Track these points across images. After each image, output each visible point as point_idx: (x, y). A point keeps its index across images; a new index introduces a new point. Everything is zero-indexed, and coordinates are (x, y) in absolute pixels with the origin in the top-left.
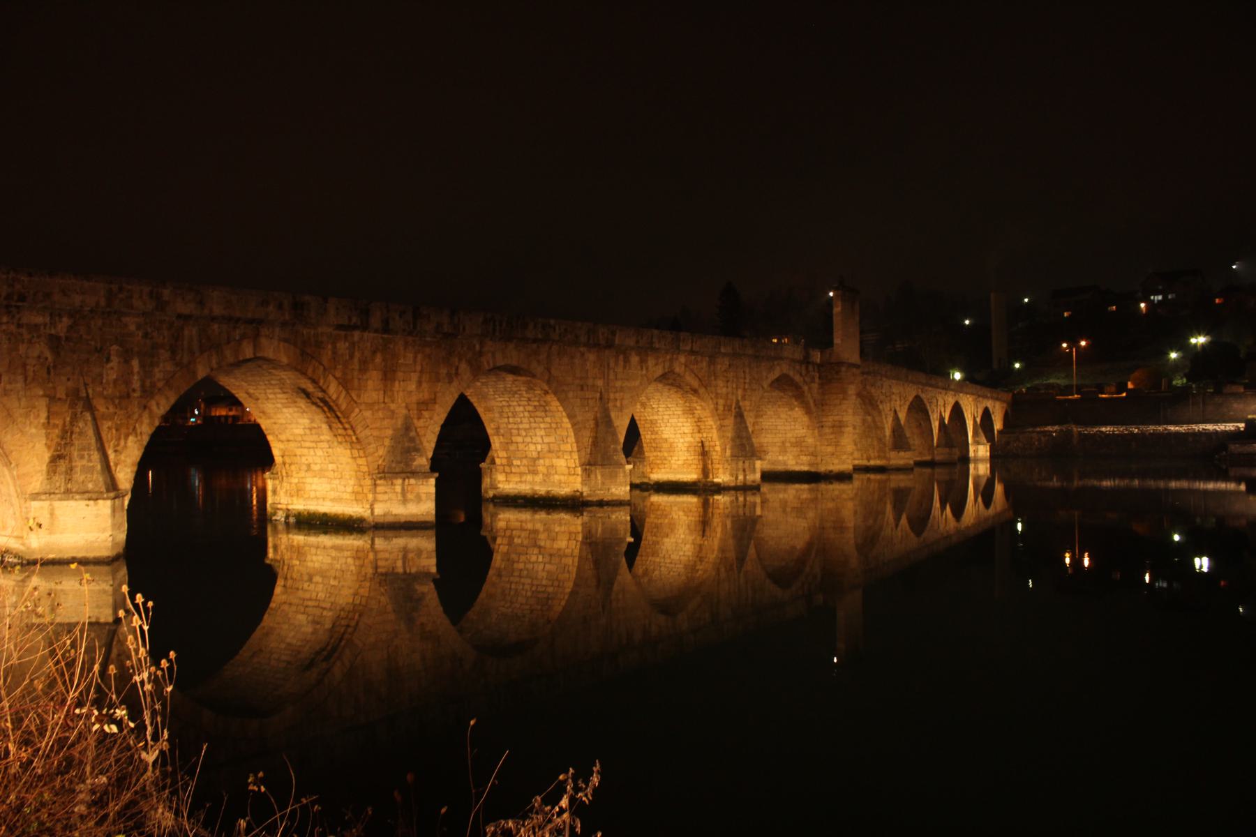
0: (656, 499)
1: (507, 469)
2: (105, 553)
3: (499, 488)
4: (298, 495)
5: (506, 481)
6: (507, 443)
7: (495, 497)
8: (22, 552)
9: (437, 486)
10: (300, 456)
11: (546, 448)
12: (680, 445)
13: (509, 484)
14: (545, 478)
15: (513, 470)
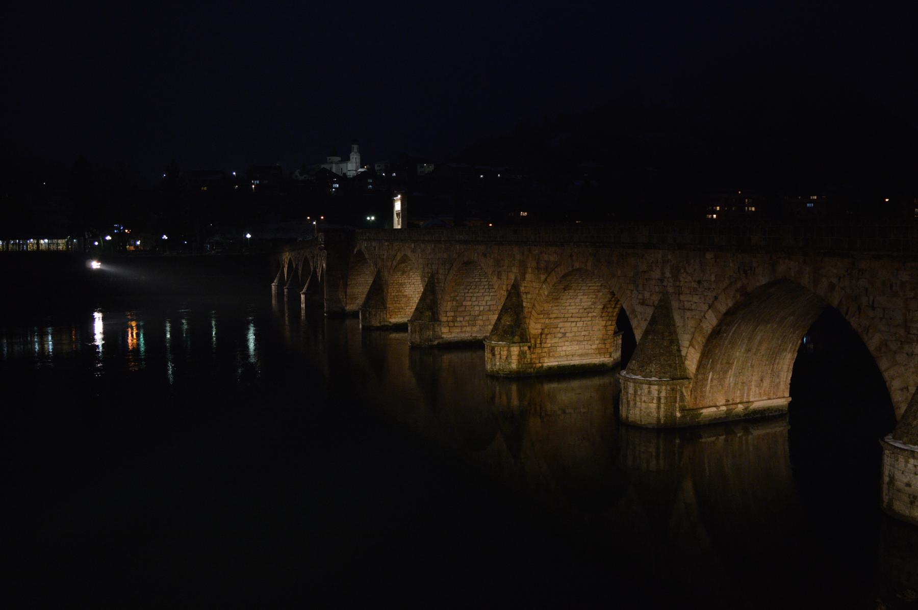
0: (394, 335)
1: (451, 324)
2: (623, 412)
3: (442, 338)
4: (549, 355)
5: (449, 332)
6: (457, 306)
7: (439, 343)
8: (782, 406)
9: (622, 339)
10: (560, 328)
11: (487, 308)
12: (415, 299)
13: (451, 334)
14: (482, 329)
15: (456, 324)
